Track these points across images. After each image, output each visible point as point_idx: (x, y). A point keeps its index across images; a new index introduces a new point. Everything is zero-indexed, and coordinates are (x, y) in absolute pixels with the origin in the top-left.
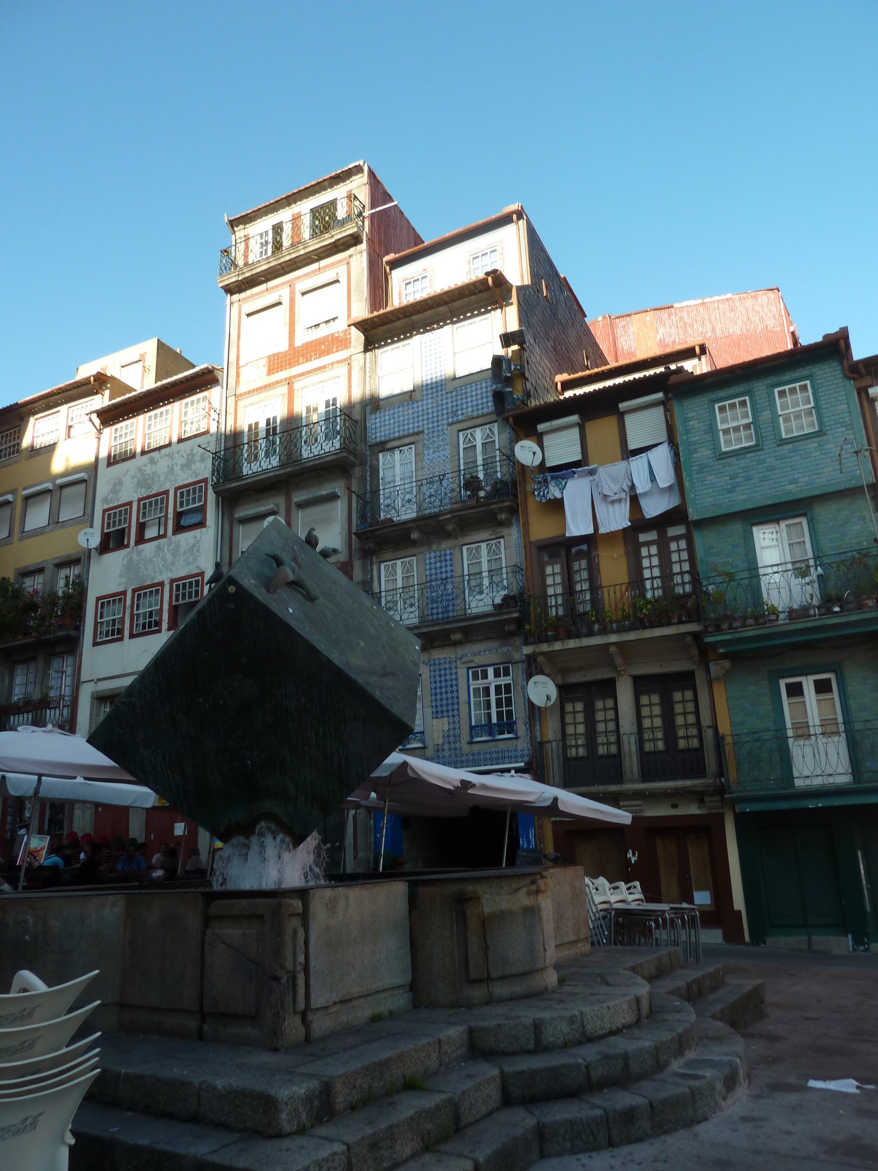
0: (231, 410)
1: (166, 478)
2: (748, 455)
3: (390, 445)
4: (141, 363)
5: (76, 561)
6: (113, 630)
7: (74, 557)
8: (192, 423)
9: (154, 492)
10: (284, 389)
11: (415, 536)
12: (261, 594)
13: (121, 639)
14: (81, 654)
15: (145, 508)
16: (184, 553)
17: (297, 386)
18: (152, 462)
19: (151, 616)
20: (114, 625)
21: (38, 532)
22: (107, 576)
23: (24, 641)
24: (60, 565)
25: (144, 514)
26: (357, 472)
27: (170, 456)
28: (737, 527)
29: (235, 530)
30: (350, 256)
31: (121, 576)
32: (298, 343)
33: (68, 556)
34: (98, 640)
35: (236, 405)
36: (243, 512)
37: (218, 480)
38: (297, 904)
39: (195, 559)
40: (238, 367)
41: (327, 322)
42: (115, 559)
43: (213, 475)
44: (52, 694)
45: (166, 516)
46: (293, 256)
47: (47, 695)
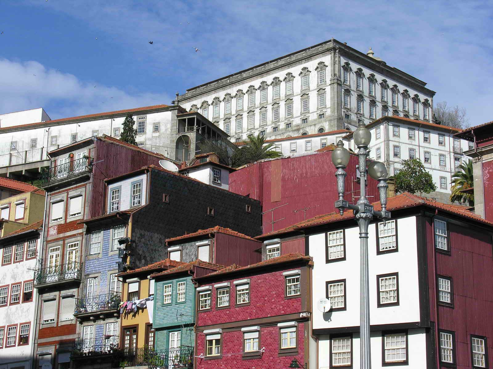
2: (169, 307)
3: (90, 276)
10: (61, 242)
11: (91, 318)
17: (66, 242)
28: (165, 331)
31: (4, 319)
32: (68, 221)
36: (47, 296)
40: (48, 228)
41: (78, 214)
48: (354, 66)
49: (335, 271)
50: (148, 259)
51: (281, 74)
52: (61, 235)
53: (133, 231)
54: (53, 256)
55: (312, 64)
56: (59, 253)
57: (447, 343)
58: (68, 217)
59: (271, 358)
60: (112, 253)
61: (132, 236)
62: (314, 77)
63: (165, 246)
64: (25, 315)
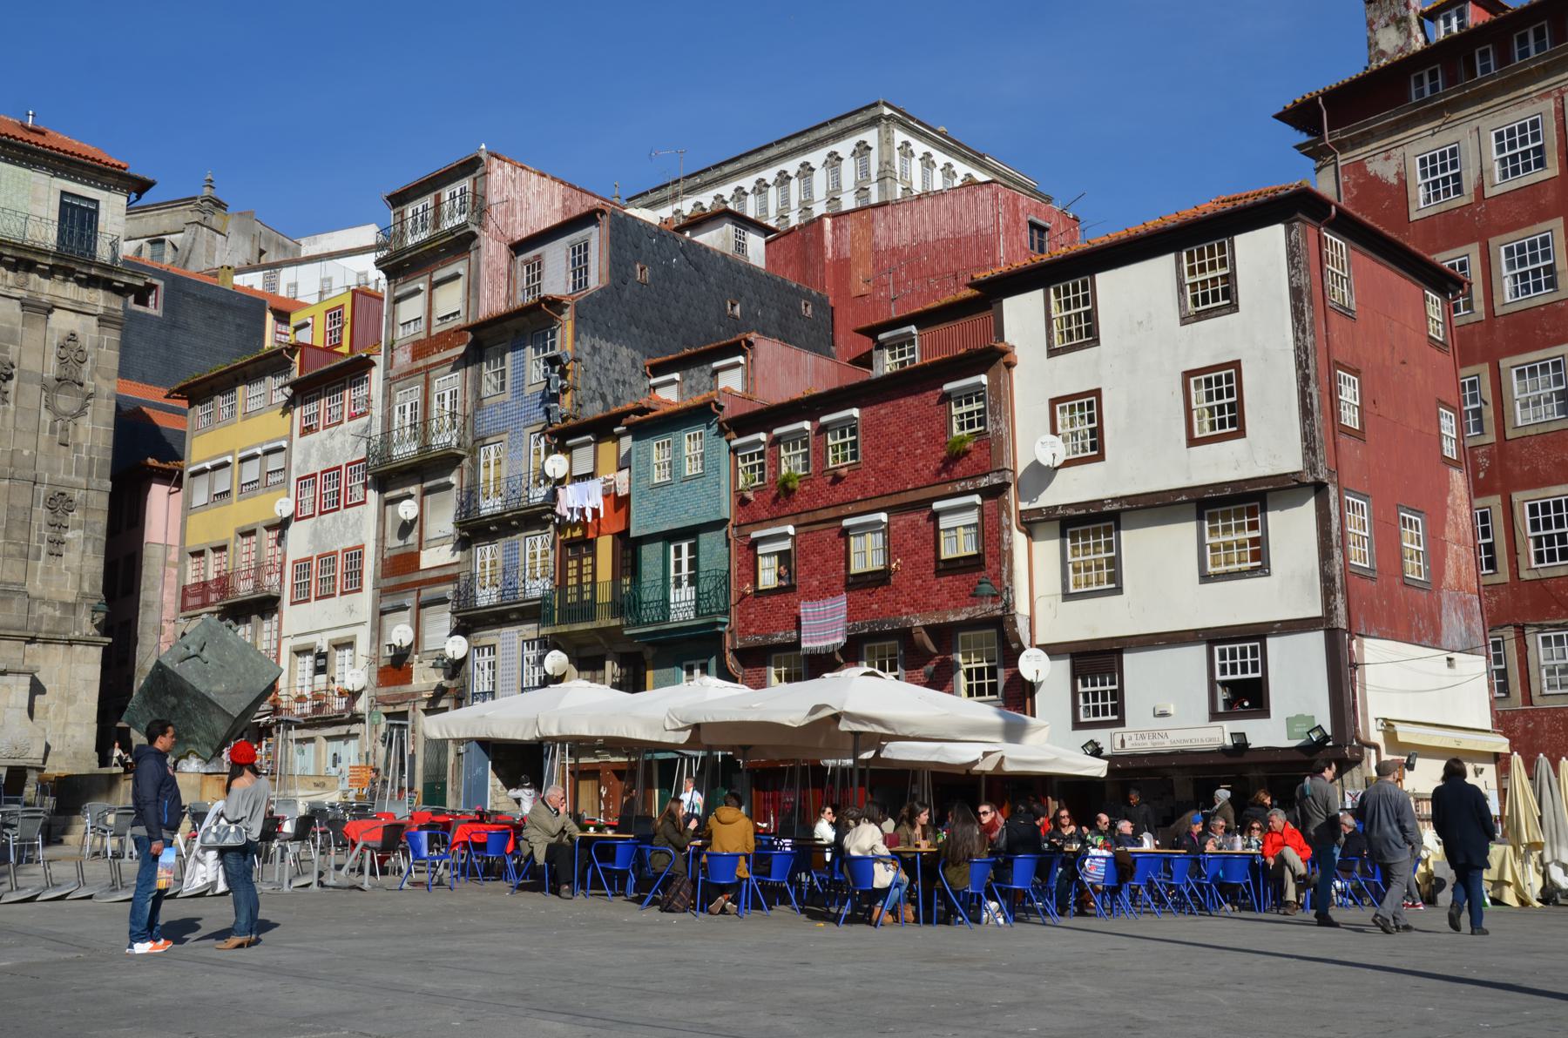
10: (422, 378)
13: (308, 601)
17: (432, 374)
26: (466, 462)
28: (660, 545)
32: (434, 331)
41: (454, 314)
48: (919, 147)
49: (1074, 372)
50: (610, 399)
51: (792, 166)
52: (420, 363)
53: (576, 338)
55: (845, 147)
57: (1358, 525)
58: (436, 322)
59: (918, 582)
60: (533, 389)
61: (575, 348)
62: (849, 169)
63: (645, 374)
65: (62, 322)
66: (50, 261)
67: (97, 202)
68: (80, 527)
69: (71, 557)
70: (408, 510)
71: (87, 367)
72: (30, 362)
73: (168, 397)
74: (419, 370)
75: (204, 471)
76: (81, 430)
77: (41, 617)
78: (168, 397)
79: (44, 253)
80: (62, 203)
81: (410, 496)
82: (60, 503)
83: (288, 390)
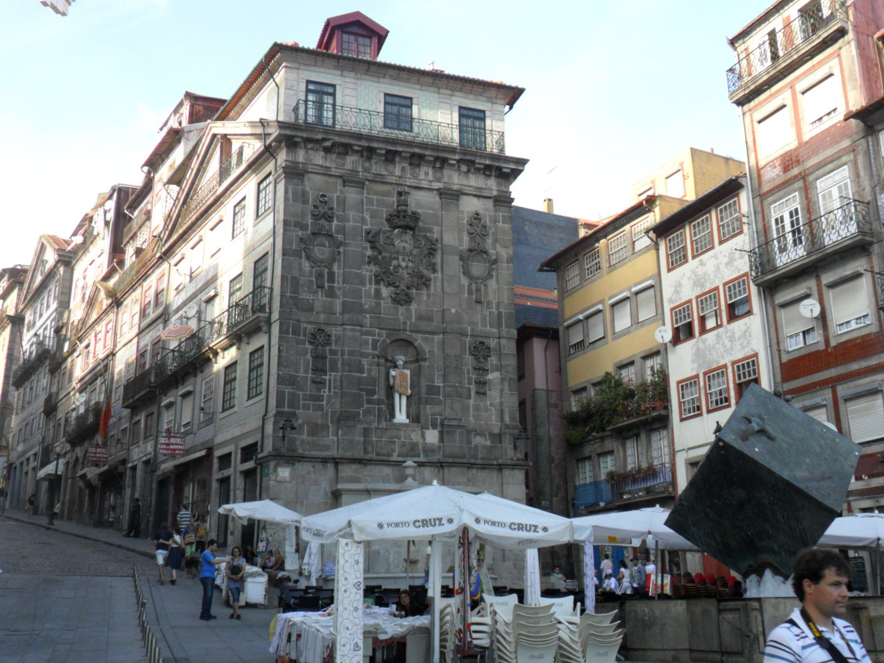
0: (759, 209)
1: (715, 276)
4: (680, 173)
5: (657, 353)
6: (694, 407)
7: (655, 350)
8: (728, 226)
9: (707, 289)
10: (800, 184)
12: (738, 444)
13: (701, 415)
14: (672, 429)
15: (702, 304)
16: (739, 339)
17: (811, 178)
18: (702, 264)
19: (721, 394)
20: (693, 403)
21: (626, 332)
22: (682, 363)
23: (629, 422)
24: (646, 357)
25: (702, 308)
27: (715, 257)
29: (778, 314)
30: (840, 48)
31: (693, 362)
33: (650, 349)
34: (684, 416)
35: (762, 204)
36: (783, 296)
37: (757, 273)
38: (756, 605)
39: (749, 343)
42: (686, 348)
43: (751, 270)
44: (656, 462)
45: (720, 308)
46: (788, 62)
47: (653, 463)
54: (782, 217)
56: (799, 207)
64: (741, 345)
65: (470, 205)
66: (457, 157)
67: (484, 112)
68: (497, 370)
69: (494, 395)
70: (810, 308)
71: (489, 241)
72: (449, 239)
73: (541, 270)
74: (795, 178)
75: (579, 321)
76: (490, 290)
77: (476, 447)
78: (541, 270)
79: (453, 150)
80: (461, 116)
81: (807, 296)
82: (481, 350)
83: (651, 234)
